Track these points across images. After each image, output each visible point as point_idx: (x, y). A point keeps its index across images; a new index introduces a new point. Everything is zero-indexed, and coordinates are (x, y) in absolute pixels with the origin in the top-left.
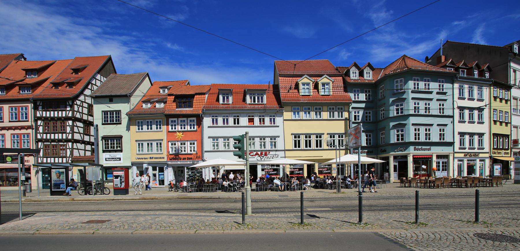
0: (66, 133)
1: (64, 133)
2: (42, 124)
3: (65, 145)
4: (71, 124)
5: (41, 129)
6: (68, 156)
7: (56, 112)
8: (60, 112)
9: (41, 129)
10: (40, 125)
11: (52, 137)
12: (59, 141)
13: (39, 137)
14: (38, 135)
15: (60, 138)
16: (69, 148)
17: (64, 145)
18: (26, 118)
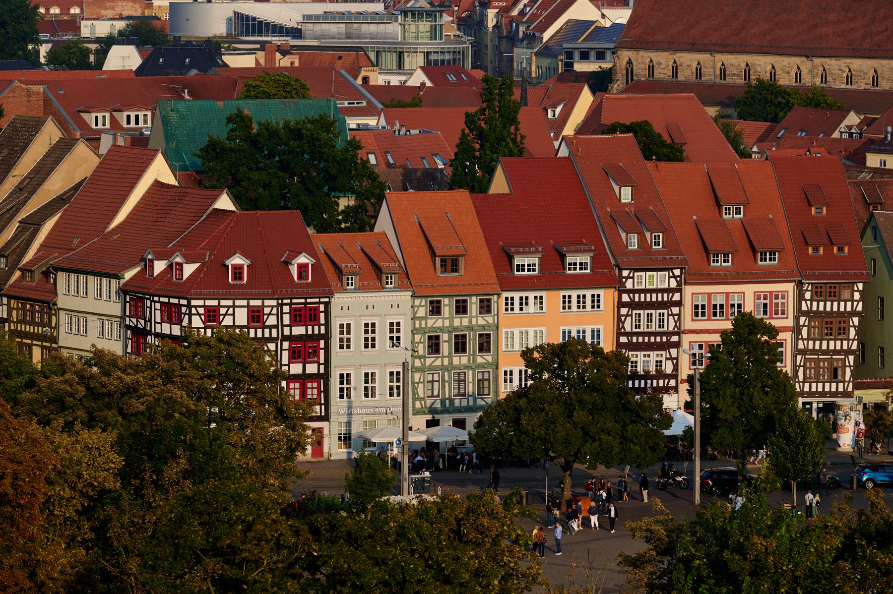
0: (848, 340)
1: (845, 339)
2: (806, 324)
3: (844, 361)
4: (856, 324)
5: (805, 331)
6: (847, 379)
7: (835, 304)
8: (842, 304)
9: (805, 331)
10: (804, 326)
11: (824, 347)
12: (836, 352)
13: (801, 346)
14: (800, 342)
15: (838, 348)
16: (850, 366)
17: (838, 360)
18: (783, 313)
